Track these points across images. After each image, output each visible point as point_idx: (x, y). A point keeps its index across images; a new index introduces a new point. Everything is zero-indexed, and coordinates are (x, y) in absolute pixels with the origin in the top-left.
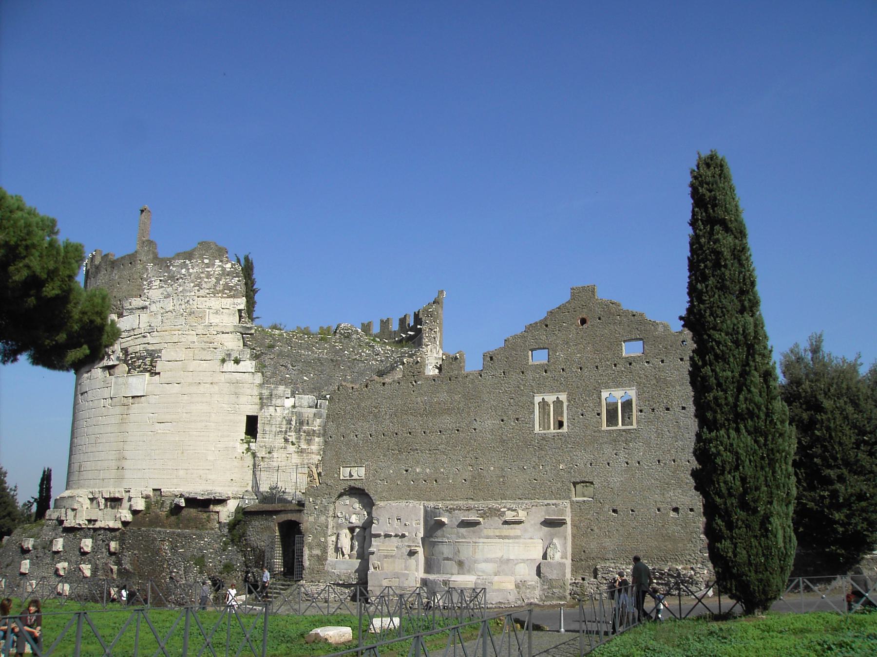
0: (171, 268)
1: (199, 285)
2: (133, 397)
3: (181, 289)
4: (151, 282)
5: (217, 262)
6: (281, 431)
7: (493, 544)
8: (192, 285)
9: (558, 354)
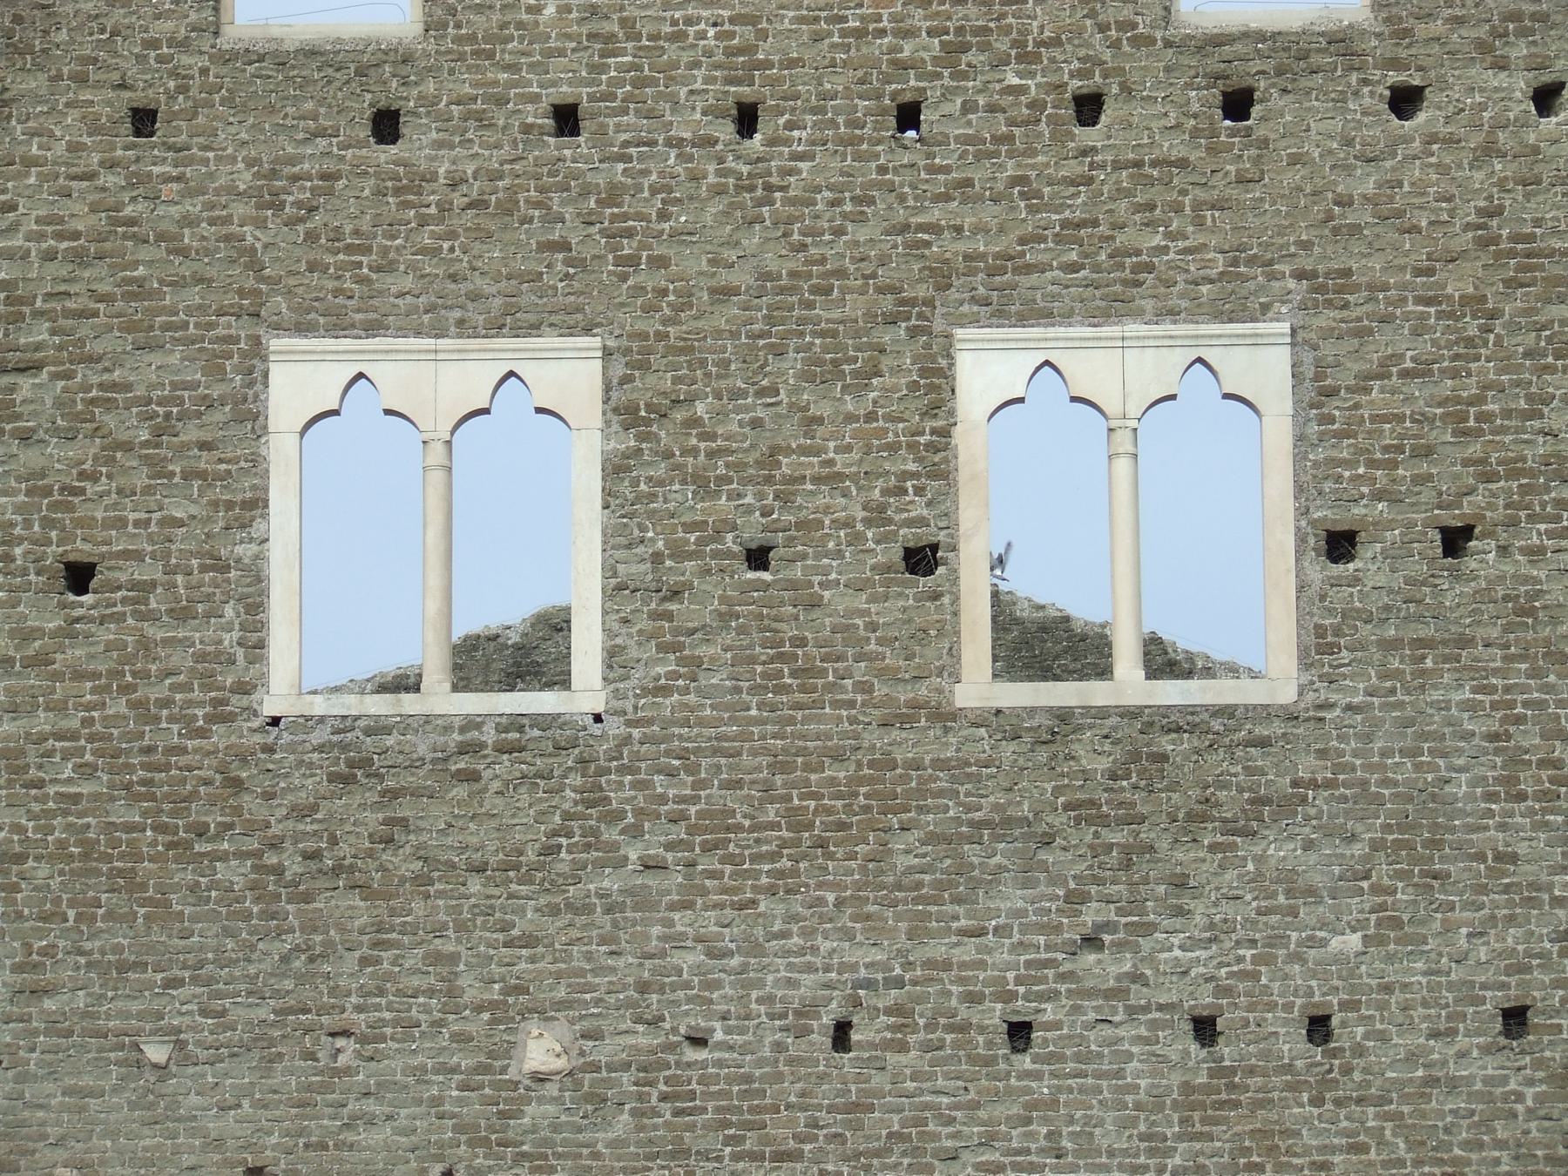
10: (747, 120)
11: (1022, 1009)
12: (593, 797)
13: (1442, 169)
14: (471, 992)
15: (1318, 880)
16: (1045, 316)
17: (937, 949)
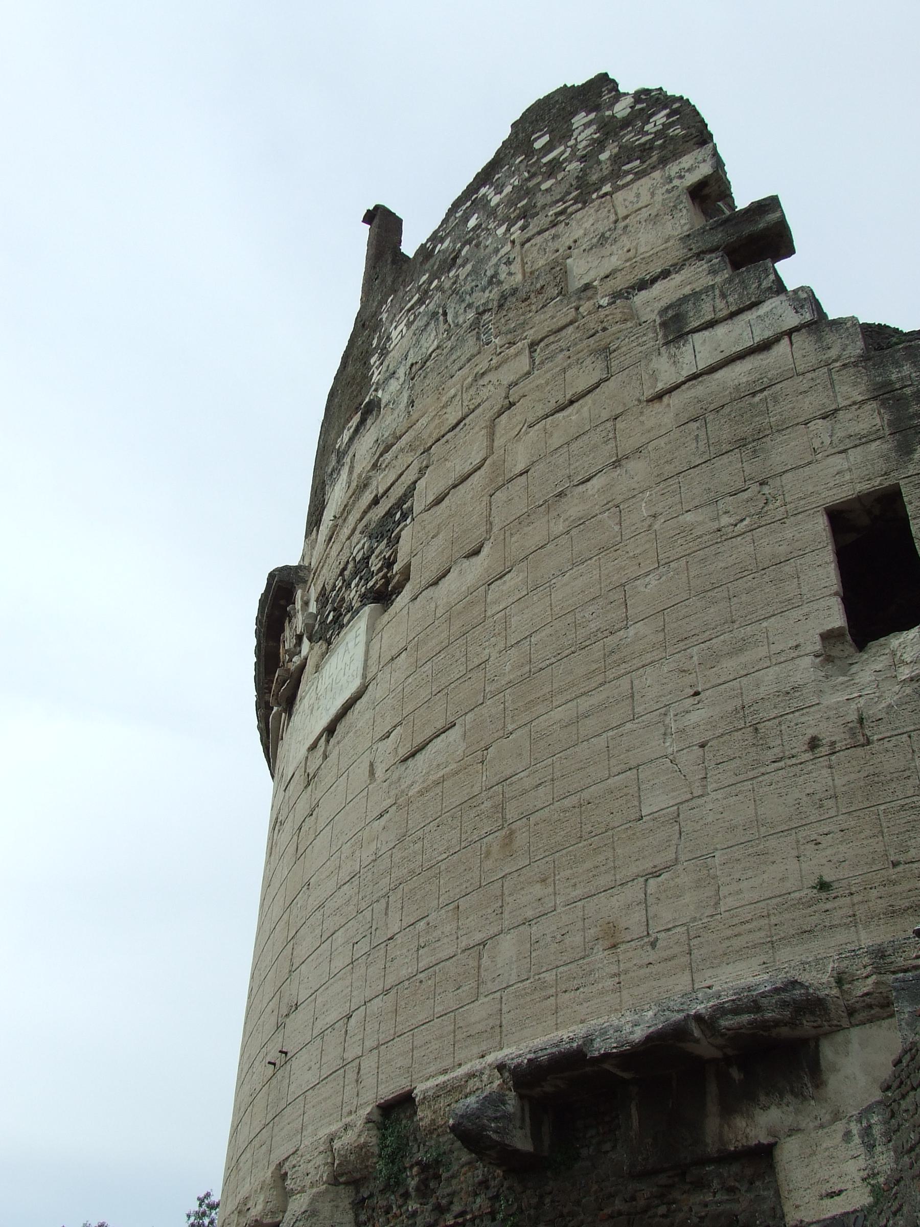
8: (501, 231)
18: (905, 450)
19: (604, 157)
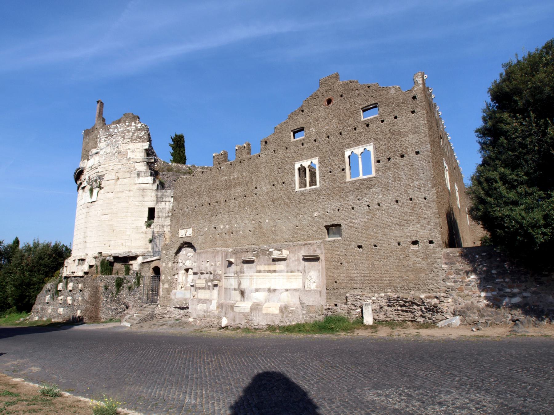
0: (110, 130)
1: (123, 137)
2: (91, 202)
3: (114, 140)
4: (101, 139)
5: (133, 124)
6: (169, 216)
7: (264, 277)
8: (120, 137)
9: (311, 130)
10: (328, 137)
11: (353, 206)
12: (319, 194)
13: (386, 127)
14: (311, 210)
15: (378, 191)
16: (352, 147)
17: (346, 202)
18: (157, 204)
19: (135, 135)
